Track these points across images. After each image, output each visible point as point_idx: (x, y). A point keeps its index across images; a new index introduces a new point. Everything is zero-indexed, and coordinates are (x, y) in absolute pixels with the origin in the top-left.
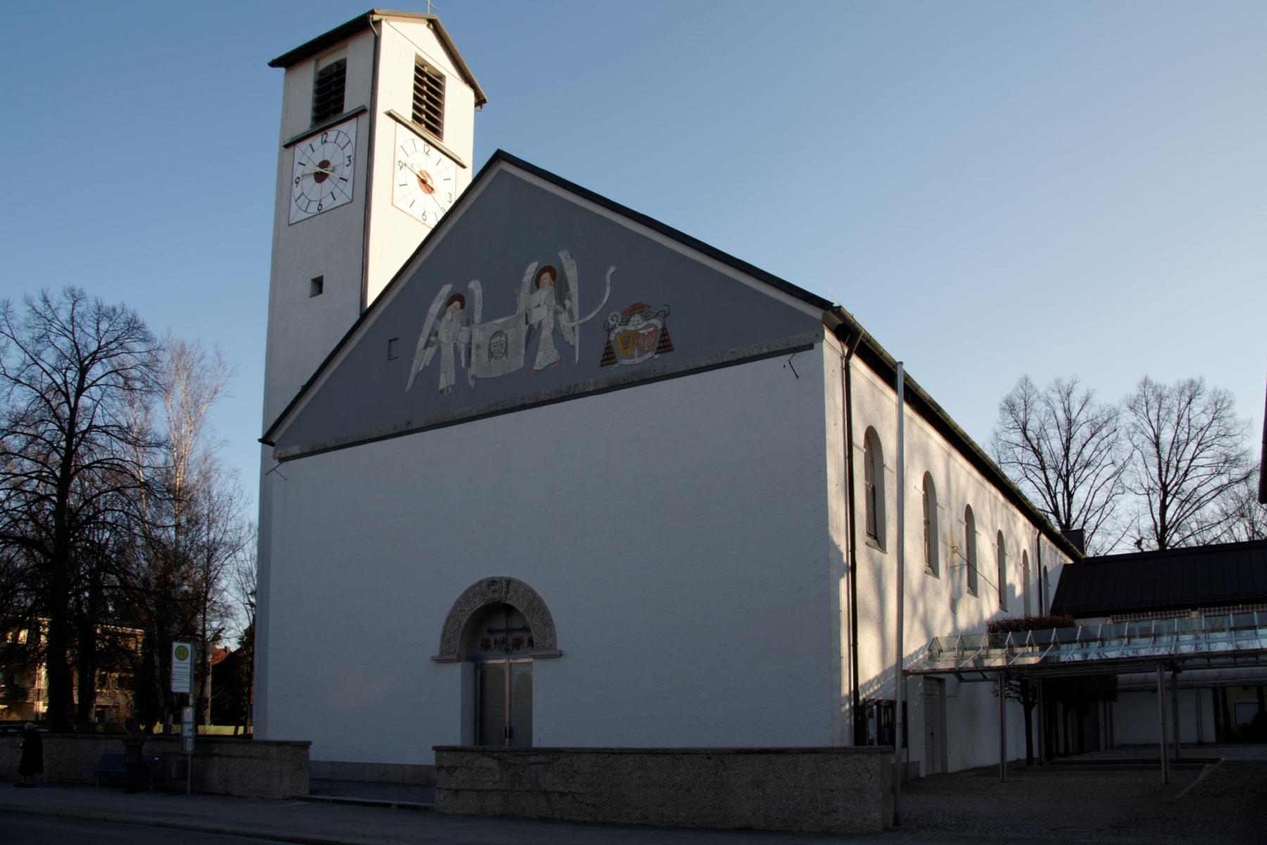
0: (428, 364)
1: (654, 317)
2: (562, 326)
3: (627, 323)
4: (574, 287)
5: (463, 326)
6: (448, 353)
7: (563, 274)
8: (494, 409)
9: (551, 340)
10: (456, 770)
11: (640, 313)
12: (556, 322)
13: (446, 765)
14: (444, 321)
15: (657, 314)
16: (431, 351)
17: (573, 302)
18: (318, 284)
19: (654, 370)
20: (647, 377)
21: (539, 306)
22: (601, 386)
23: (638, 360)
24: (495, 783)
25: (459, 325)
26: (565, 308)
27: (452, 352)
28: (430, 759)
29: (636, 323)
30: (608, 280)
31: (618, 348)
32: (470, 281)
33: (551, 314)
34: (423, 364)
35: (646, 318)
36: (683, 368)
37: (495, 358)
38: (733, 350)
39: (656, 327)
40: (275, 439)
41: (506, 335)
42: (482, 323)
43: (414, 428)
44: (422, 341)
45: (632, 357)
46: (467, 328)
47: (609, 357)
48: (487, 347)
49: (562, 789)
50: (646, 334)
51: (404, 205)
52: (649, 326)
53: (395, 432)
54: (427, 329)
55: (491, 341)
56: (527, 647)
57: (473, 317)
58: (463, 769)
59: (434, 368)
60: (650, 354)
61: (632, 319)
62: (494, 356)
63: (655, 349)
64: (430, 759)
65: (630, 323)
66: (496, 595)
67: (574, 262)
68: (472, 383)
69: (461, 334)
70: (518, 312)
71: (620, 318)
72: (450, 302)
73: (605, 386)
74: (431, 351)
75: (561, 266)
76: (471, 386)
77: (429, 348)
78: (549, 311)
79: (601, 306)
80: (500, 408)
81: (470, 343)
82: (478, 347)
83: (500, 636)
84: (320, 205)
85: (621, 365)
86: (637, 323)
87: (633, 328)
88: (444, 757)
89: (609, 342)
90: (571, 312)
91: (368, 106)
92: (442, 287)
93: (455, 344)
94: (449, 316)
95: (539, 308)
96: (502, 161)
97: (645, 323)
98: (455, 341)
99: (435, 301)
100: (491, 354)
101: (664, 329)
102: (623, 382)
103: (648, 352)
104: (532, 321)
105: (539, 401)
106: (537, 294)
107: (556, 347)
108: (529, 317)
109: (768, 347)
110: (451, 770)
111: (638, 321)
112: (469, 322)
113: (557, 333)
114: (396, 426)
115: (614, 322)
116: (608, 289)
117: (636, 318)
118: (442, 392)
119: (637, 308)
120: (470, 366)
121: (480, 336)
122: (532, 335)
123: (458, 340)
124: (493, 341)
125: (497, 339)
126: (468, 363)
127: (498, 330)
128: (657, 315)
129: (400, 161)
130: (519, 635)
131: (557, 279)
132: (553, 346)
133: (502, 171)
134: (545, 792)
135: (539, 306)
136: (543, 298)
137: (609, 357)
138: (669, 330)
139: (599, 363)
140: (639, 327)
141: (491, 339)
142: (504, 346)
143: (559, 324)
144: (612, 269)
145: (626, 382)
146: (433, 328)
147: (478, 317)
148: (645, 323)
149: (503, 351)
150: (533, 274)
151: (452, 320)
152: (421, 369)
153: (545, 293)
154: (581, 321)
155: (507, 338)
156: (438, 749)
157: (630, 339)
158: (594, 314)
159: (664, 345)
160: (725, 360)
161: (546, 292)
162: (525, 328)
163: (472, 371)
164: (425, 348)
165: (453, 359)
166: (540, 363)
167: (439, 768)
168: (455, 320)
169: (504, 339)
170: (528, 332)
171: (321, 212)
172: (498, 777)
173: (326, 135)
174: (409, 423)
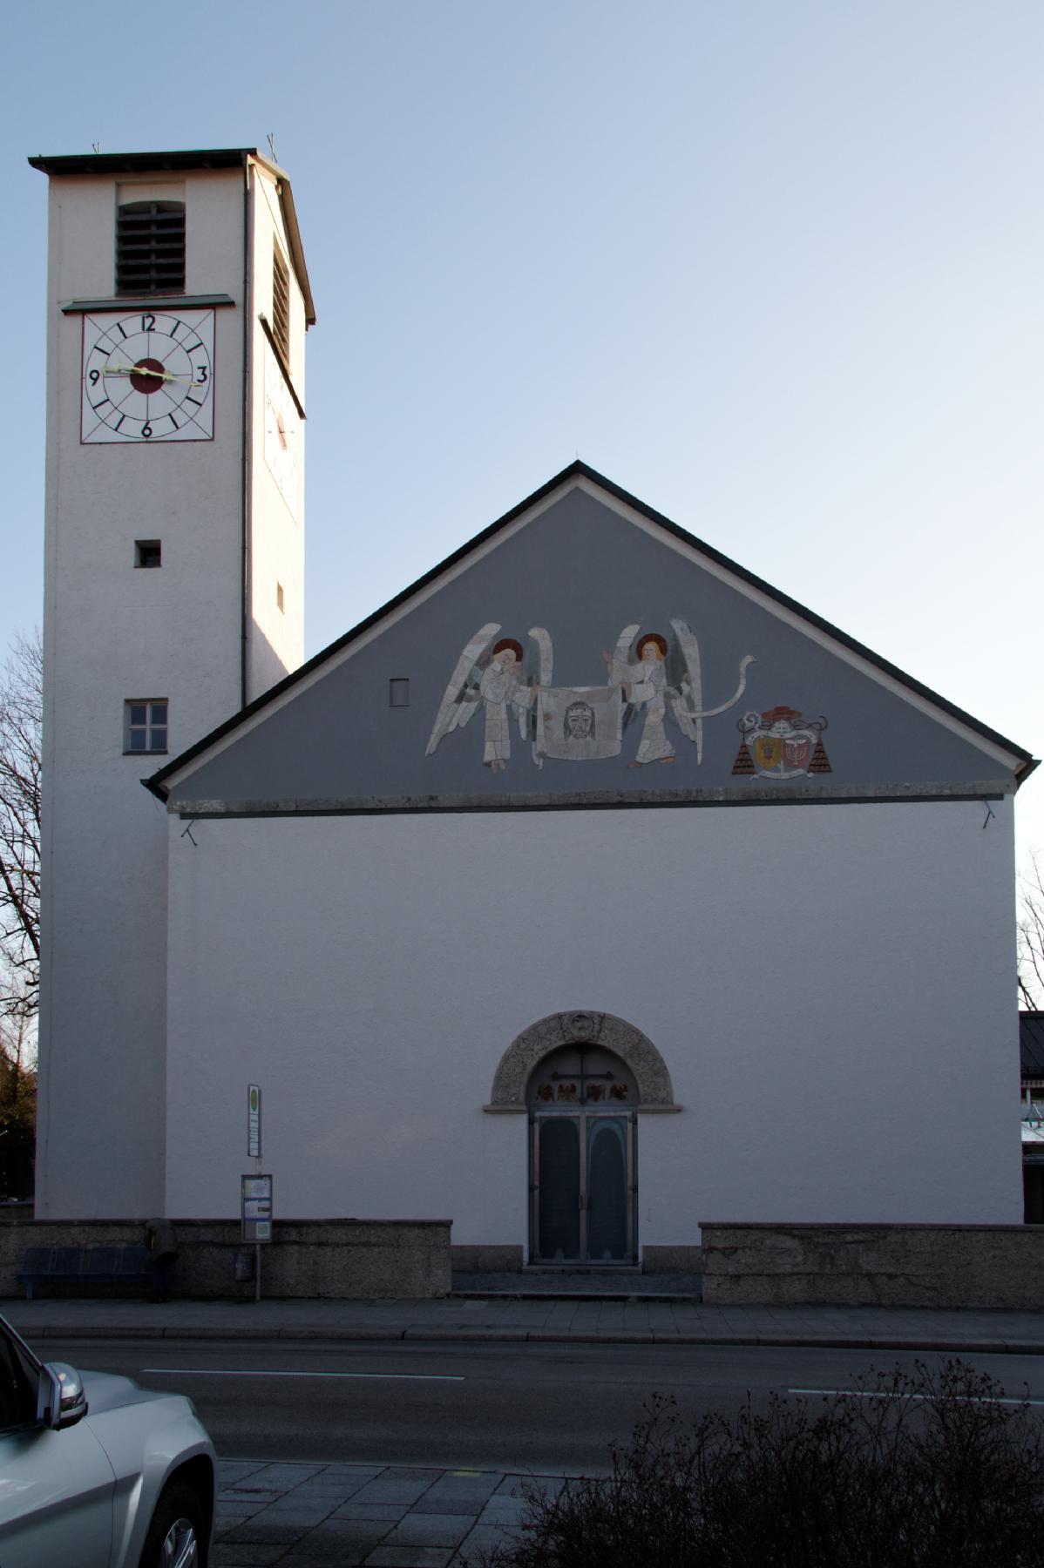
0: (463, 724)
1: (807, 728)
3: (770, 727)
4: (694, 668)
5: (521, 684)
7: (677, 649)
8: (575, 800)
9: (661, 728)
11: (788, 719)
12: (669, 709)
15: (810, 725)
16: (468, 709)
19: (807, 791)
20: (798, 797)
21: (642, 682)
22: (734, 797)
23: (785, 776)
24: (796, 1265)
25: (514, 682)
26: (681, 693)
27: (504, 716)
28: (694, 1239)
29: (782, 730)
31: (757, 756)
32: (529, 628)
35: (795, 727)
36: (844, 795)
37: (575, 736)
38: (908, 784)
39: (809, 740)
40: (171, 784)
41: (592, 709)
42: (553, 685)
43: (441, 806)
44: (452, 691)
45: (776, 770)
46: (529, 689)
47: (744, 764)
48: (562, 719)
52: (800, 737)
53: (407, 805)
54: (459, 677)
55: (567, 712)
56: (610, 1098)
57: (538, 677)
59: (474, 731)
60: (801, 771)
61: (777, 725)
63: (807, 766)
64: (694, 1239)
65: (774, 729)
66: (583, 1034)
67: (694, 638)
68: (540, 763)
69: (518, 694)
70: (610, 683)
71: (760, 720)
72: (501, 645)
73: (740, 798)
74: (468, 709)
75: (675, 638)
77: (464, 704)
78: (657, 691)
80: (585, 801)
81: (534, 708)
82: (547, 717)
83: (567, 1083)
84: (146, 427)
85: (761, 776)
86: (781, 730)
87: (778, 736)
88: (717, 1236)
89: (744, 746)
90: (689, 700)
91: (237, 297)
92: (483, 626)
93: (509, 707)
94: (496, 665)
96: (581, 476)
97: (794, 733)
98: (509, 703)
99: (472, 641)
101: (819, 744)
102: (765, 798)
103: (796, 767)
104: (632, 700)
105: (645, 801)
106: (639, 666)
107: (667, 738)
109: (950, 789)
110: (729, 1252)
112: (532, 681)
113: (670, 720)
115: (753, 724)
116: (743, 682)
118: (488, 764)
119: (782, 713)
120: (534, 739)
122: (633, 716)
123: (512, 701)
124: (571, 714)
127: (578, 700)
128: (810, 726)
130: (598, 1083)
131: (669, 654)
132: (664, 736)
133: (577, 489)
134: (869, 1275)
135: (642, 682)
136: (648, 673)
137: (744, 764)
138: (826, 748)
139: (731, 769)
141: (567, 712)
142: (589, 723)
143: (673, 711)
144: (748, 659)
145: (769, 798)
146: (470, 677)
147: (546, 677)
149: (588, 729)
150: (631, 640)
152: (451, 728)
153: (652, 668)
154: (706, 714)
155: (593, 714)
156: (705, 1227)
157: (774, 749)
158: (722, 709)
159: (820, 763)
160: (898, 794)
161: (652, 665)
162: (621, 708)
163: (539, 746)
165: (506, 725)
166: (644, 754)
168: (507, 674)
169: (588, 713)
170: (625, 713)
171: (149, 439)
172: (800, 1258)
173: (150, 320)
174: (432, 798)
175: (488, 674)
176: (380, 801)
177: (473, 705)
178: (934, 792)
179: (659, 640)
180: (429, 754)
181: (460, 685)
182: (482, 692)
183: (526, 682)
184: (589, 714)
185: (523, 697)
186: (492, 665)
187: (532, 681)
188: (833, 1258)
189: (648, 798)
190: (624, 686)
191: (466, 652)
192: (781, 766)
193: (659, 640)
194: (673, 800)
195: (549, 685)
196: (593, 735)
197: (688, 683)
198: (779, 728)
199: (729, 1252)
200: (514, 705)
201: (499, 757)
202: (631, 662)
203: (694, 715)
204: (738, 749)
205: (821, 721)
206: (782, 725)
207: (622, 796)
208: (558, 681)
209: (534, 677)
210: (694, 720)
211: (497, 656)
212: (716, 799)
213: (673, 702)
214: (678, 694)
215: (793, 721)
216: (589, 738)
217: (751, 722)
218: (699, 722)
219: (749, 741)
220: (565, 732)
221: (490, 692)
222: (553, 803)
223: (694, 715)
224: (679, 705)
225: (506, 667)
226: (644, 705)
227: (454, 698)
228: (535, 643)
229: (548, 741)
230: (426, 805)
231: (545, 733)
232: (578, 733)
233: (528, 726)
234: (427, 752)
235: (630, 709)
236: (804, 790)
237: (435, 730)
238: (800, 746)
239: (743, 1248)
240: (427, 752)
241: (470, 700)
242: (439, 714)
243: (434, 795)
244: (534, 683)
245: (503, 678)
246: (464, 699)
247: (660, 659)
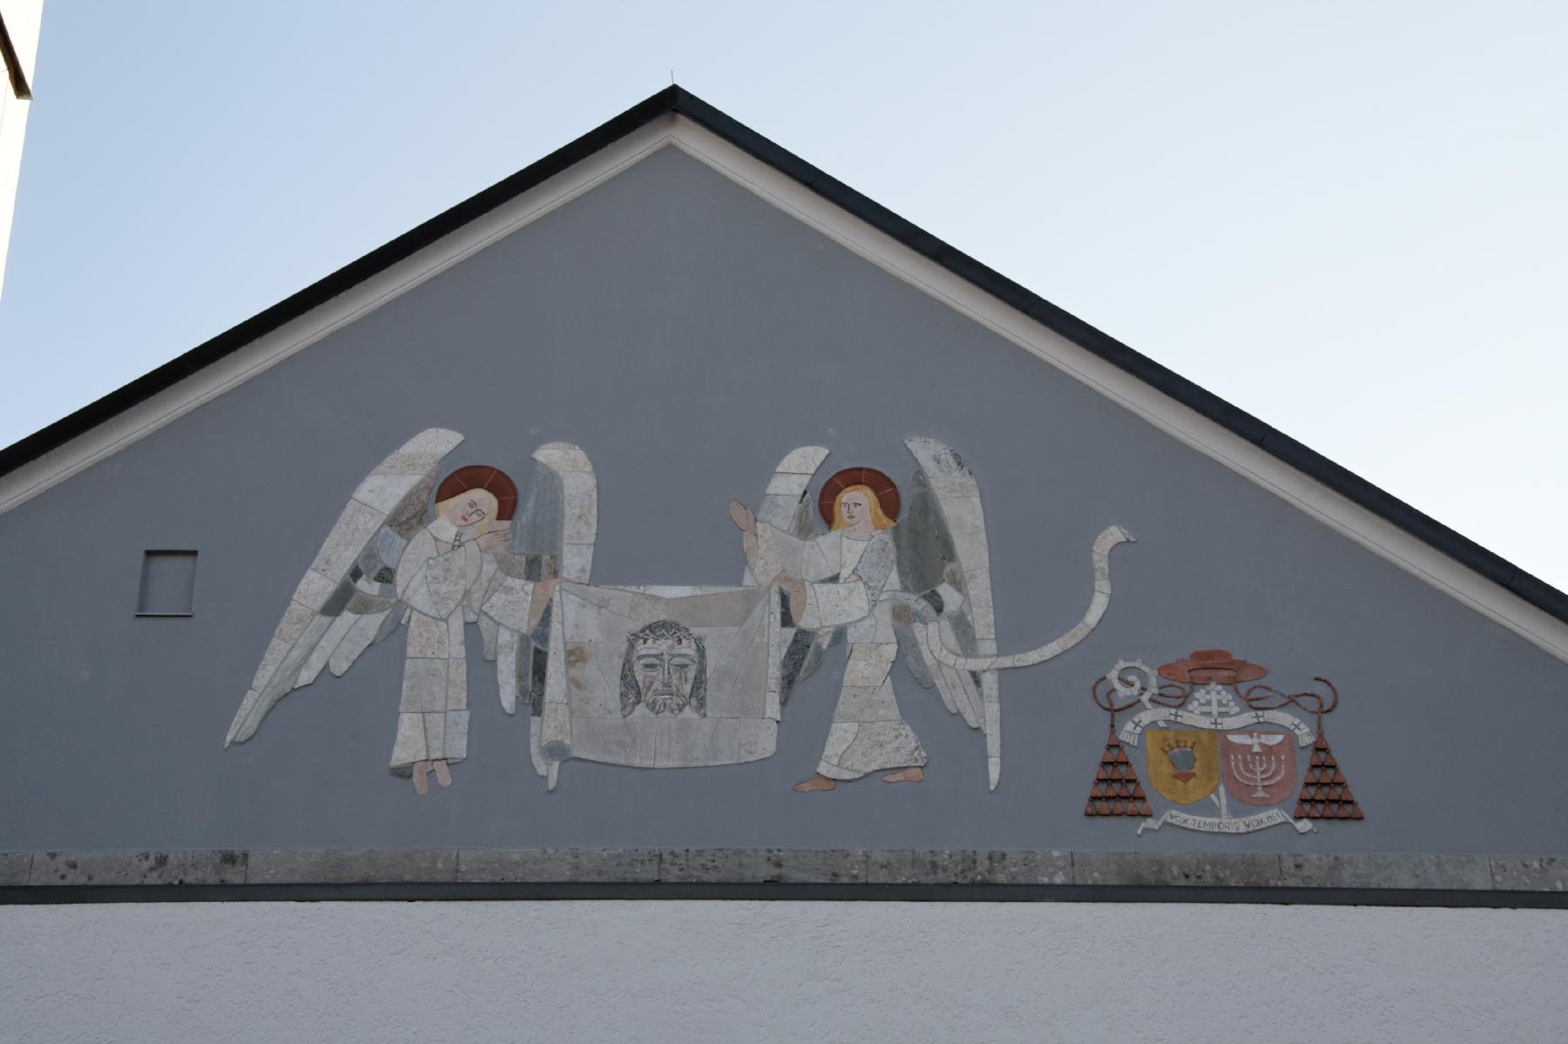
0: (339, 667)
1: (1282, 707)
3: (1183, 701)
5: (509, 571)
7: (927, 506)
8: (649, 873)
9: (887, 693)
11: (1231, 683)
12: (907, 647)
19: (1298, 866)
20: (1272, 883)
22: (1095, 877)
25: (490, 568)
26: (939, 609)
27: (457, 649)
29: (1215, 709)
31: (1152, 771)
33: (884, 616)
34: (316, 663)
35: (1251, 703)
36: (1407, 882)
37: (652, 706)
44: (316, 585)
46: (530, 586)
48: (618, 663)
50: (1256, 749)
52: (1272, 728)
53: (153, 879)
55: (632, 646)
60: (1277, 815)
61: (1200, 694)
62: (650, 697)
67: (971, 481)
68: (550, 771)
69: (498, 599)
70: (748, 580)
71: (1153, 681)
72: (455, 482)
73: (1112, 880)
75: (920, 478)
76: (545, 778)
77: (347, 617)
79: (1079, 632)
80: (673, 875)
81: (542, 633)
82: (576, 656)
85: (1165, 824)
87: (1205, 723)
89: (1115, 746)
90: (962, 626)
93: (471, 628)
94: (445, 523)
95: (831, 586)
96: (682, 118)
97: (1248, 718)
98: (472, 618)
99: (380, 468)
100: (631, 689)
101: (1320, 748)
102: (1183, 882)
103: (1265, 804)
104: (806, 621)
105: (845, 880)
106: (827, 541)
107: (905, 716)
108: (793, 605)
111: (1220, 704)
115: (1135, 691)
118: (404, 773)
120: (538, 710)
124: (642, 649)
125: (663, 646)
127: (663, 617)
128: (1290, 702)
131: (904, 515)
132: (895, 713)
133: (671, 148)
135: (834, 579)
136: (851, 560)
138: (1339, 755)
139: (1083, 803)
140: (1228, 723)
141: (632, 646)
142: (692, 673)
145: (1192, 882)
146: (370, 554)
147: (576, 559)
149: (688, 688)
150: (806, 480)
151: (457, 544)
152: (306, 677)
154: (1007, 662)
155: (701, 651)
158: (1051, 650)
162: (779, 640)
163: (549, 727)
165: (460, 674)
168: (472, 548)
169: (688, 648)
170: (790, 653)
174: (229, 859)
175: (422, 542)
176: (74, 866)
177: (372, 623)
179: (878, 482)
180: (233, 743)
181: (341, 571)
182: (399, 590)
183: (522, 569)
184: (692, 652)
186: (432, 526)
189: (854, 871)
190: (785, 588)
191: (364, 492)
192: (1221, 798)
193: (878, 482)
194: (923, 880)
195: (586, 577)
196: (702, 703)
198: (1209, 703)
200: (484, 623)
201: (438, 755)
202: (804, 530)
203: (973, 664)
204: (1100, 754)
205: (1320, 689)
206: (1214, 697)
207: (779, 865)
208: (607, 570)
209: (546, 558)
210: (976, 677)
211: (442, 505)
212: (1046, 880)
213: (918, 627)
214: (931, 611)
215: (1243, 688)
216: (688, 712)
217: (1131, 685)
218: (989, 681)
219: (1128, 732)
221: (424, 589)
222: (583, 879)
223: (973, 664)
224: (934, 639)
225: (470, 533)
226: (839, 635)
227: (320, 602)
228: (551, 479)
230: (212, 879)
231: (569, 695)
232: (660, 698)
233: (520, 677)
234: (229, 738)
235: (802, 642)
236: (1288, 864)
237: (262, 678)
238: (1268, 750)
240: (229, 738)
241: (365, 607)
242: (275, 642)
244: (545, 571)
245: (459, 558)
246: (350, 604)
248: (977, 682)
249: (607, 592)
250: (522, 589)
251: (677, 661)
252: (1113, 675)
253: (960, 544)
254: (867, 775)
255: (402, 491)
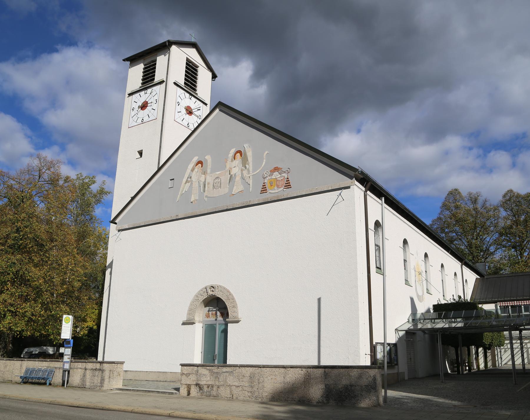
2: (245, 176)
4: (250, 159)
6: (195, 185)
7: (245, 154)
8: (214, 211)
10: (190, 375)
12: (242, 174)
13: (185, 373)
14: (194, 172)
16: (188, 185)
17: (250, 166)
18: (141, 153)
21: (235, 167)
22: (261, 202)
23: (276, 191)
25: (200, 174)
26: (246, 168)
28: (178, 369)
29: (276, 175)
30: (264, 157)
31: (268, 186)
38: (317, 188)
42: (211, 173)
47: (264, 190)
49: (237, 384)
50: (280, 180)
51: (179, 120)
52: (281, 177)
57: (207, 171)
58: (193, 374)
59: (189, 193)
60: (282, 189)
61: (274, 173)
63: (284, 187)
64: (178, 369)
65: (273, 175)
68: (206, 199)
71: (269, 173)
75: (245, 150)
77: (187, 183)
79: (261, 168)
81: (205, 182)
82: (208, 184)
86: (276, 175)
92: (194, 157)
94: (196, 170)
97: (280, 176)
101: (288, 178)
103: (281, 187)
104: (231, 174)
106: (234, 162)
108: (230, 171)
110: (188, 375)
112: (205, 173)
113: (243, 178)
114: (171, 217)
116: (265, 160)
117: (276, 173)
119: (276, 169)
120: (205, 192)
121: (210, 179)
125: (217, 180)
126: (204, 191)
129: (178, 102)
135: (235, 167)
137: (264, 190)
138: (289, 179)
139: (260, 192)
140: (277, 177)
142: (220, 183)
143: (243, 176)
144: (266, 152)
145: (271, 200)
146: (189, 175)
147: (209, 171)
148: (280, 176)
152: (183, 192)
154: (253, 174)
155: (221, 180)
156: (183, 365)
157: (274, 183)
159: (288, 185)
163: (206, 194)
164: (186, 183)
167: (182, 374)
168: (199, 172)
172: (209, 378)
177: (189, 184)
178: (326, 190)
179: (240, 152)
180: (177, 202)
184: (220, 180)
185: (202, 179)
186: (195, 170)
187: (205, 173)
188: (219, 379)
192: (276, 188)
196: (221, 187)
197: (248, 164)
199: (188, 375)
203: (249, 175)
204: (262, 184)
205: (289, 170)
206: (276, 173)
209: (206, 171)
218: (251, 177)
220: (213, 188)
223: (249, 175)
226: (235, 174)
229: (210, 192)
233: (203, 188)
236: (282, 195)
237: (179, 194)
239: (192, 374)
243: (177, 214)
244: (206, 173)
247: (240, 158)
248: (250, 178)
249: (212, 175)
250: (203, 176)
251: (219, 182)
252: (265, 173)
253: (249, 158)
254: (237, 193)
255: (192, 166)
